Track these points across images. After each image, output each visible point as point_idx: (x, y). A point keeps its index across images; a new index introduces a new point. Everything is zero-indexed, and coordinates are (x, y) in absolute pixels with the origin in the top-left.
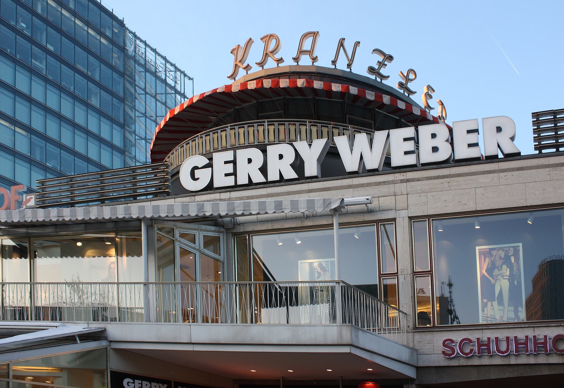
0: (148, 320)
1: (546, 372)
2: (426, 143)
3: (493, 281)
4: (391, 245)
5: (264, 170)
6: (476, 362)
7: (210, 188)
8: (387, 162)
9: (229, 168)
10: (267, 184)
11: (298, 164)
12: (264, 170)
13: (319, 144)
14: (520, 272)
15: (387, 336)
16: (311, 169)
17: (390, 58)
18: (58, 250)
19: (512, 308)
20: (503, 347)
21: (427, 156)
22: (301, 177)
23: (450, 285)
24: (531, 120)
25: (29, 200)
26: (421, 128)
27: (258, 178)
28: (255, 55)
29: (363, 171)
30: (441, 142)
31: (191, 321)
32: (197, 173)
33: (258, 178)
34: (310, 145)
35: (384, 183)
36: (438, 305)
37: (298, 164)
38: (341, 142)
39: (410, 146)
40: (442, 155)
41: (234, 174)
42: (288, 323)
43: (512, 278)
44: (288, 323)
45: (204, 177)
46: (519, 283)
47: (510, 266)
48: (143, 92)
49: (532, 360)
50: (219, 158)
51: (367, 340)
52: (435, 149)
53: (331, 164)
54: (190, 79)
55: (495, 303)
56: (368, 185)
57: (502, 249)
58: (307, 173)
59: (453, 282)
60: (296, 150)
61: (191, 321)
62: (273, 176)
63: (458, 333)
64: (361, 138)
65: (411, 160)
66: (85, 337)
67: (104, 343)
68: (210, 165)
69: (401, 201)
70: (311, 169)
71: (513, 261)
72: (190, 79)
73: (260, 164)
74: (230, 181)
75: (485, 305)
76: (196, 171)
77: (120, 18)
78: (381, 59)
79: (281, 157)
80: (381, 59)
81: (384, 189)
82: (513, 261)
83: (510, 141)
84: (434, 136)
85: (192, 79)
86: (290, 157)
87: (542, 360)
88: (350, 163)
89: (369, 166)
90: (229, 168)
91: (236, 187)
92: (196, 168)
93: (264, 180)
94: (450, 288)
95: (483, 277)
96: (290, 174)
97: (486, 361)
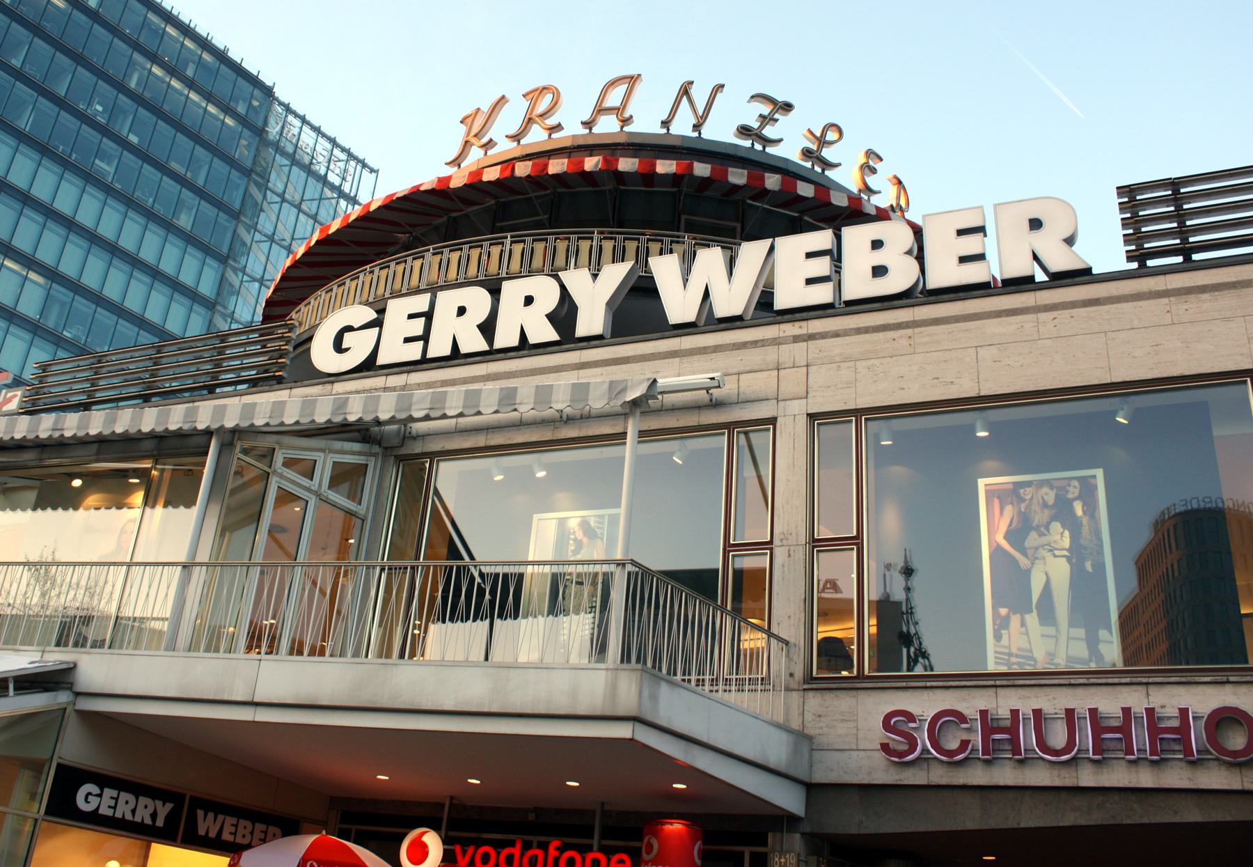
0: (172, 647)
1: (1192, 814)
3: (1023, 562)
4: (759, 477)
5: (487, 328)
6: (978, 776)
7: (369, 366)
10: (492, 354)
11: (565, 315)
12: (487, 328)
13: (615, 274)
14: (1101, 540)
15: (733, 697)
16: (591, 320)
17: (787, 107)
18: (32, 496)
19: (1080, 632)
20: (1058, 737)
21: (857, 284)
23: (908, 572)
24: (1114, 201)
25: (10, 400)
26: (847, 232)
28: (509, 120)
29: (708, 321)
31: (264, 649)
33: (473, 342)
34: (595, 276)
35: (755, 344)
36: (874, 621)
37: (565, 315)
38: (665, 269)
39: (822, 266)
42: (487, 659)
43: (1076, 555)
44: (487, 659)
45: (359, 346)
46: (1099, 567)
47: (1072, 525)
48: (278, 199)
49: (1145, 778)
50: (398, 310)
51: (681, 707)
52: (879, 271)
53: (638, 311)
54: (372, 171)
55: (1032, 619)
56: (717, 349)
57: (1048, 483)
58: (581, 330)
59: (915, 564)
60: (563, 288)
61: (264, 649)
62: (506, 337)
63: (926, 695)
64: (710, 259)
65: (823, 294)
66: (28, 682)
67: (63, 697)
69: (792, 381)
70: (591, 320)
71: (1079, 512)
72: (372, 171)
73: (482, 316)
75: (1002, 624)
76: (347, 336)
77: (269, 83)
78: (766, 109)
80: (766, 109)
81: (754, 357)
82: (1079, 512)
83: (1065, 246)
85: (377, 172)
87: (1176, 777)
88: (679, 304)
89: (721, 311)
91: (424, 362)
92: (349, 329)
93: (485, 347)
94: (907, 580)
95: (996, 552)
96: (543, 332)
97: (1006, 775)
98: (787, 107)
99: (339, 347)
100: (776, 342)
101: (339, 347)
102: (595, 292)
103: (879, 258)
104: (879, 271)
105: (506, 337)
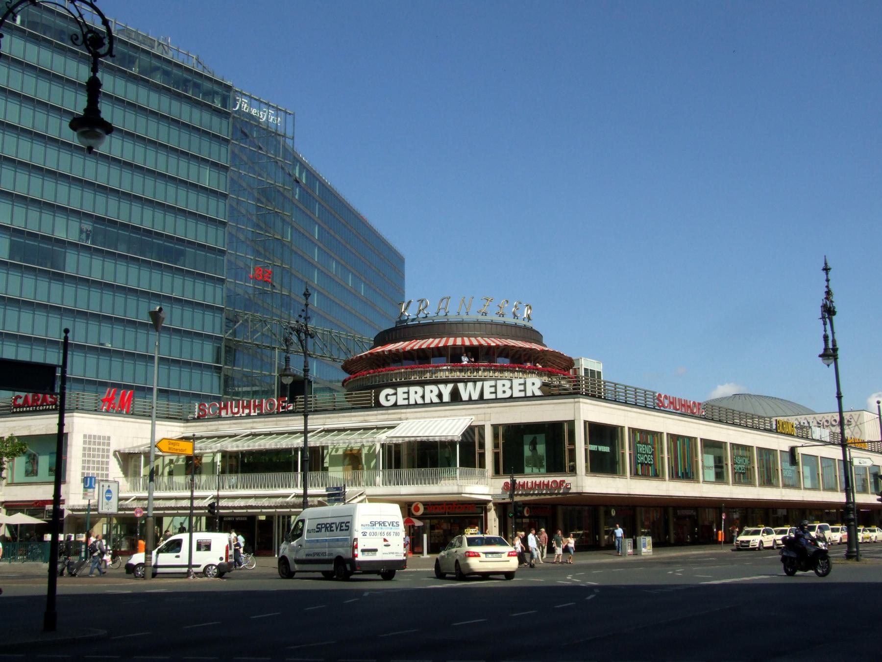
2: (500, 389)
7: (395, 406)
9: (406, 396)
10: (424, 405)
11: (440, 396)
12: (423, 397)
13: (450, 386)
16: (446, 398)
21: (500, 395)
22: (442, 403)
29: (470, 401)
30: (507, 388)
32: (389, 398)
33: (420, 401)
37: (440, 396)
40: (508, 395)
41: (408, 399)
45: (392, 400)
53: (456, 397)
62: (427, 401)
68: (395, 394)
74: (406, 402)
79: (432, 391)
81: (480, 411)
84: (504, 385)
86: (436, 392)
88: (465, 397)
90: (406, 396)
99: (388, 400)
101: (388, 400)
102: (447, 390)
103: (504, 389)
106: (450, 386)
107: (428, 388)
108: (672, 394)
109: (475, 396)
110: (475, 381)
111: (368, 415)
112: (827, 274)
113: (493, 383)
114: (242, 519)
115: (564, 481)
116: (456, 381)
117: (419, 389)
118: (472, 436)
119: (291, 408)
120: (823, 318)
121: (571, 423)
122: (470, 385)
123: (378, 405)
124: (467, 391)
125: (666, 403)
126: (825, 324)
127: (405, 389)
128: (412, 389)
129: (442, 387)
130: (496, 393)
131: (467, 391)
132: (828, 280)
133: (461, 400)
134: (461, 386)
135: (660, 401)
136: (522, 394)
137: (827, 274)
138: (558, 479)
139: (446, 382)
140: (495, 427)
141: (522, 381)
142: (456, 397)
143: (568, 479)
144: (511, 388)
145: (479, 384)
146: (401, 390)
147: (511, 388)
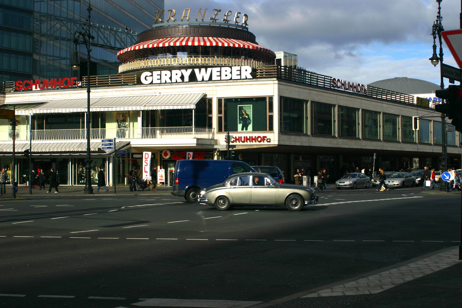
1: (255, 147)
2: (223, 73)
5: (171, 78)
7: (152, 83)
8: (210, 79)
11: (182, 77)
12: (171, 78)
13: (190, 71)
16: (186, 79)
21: (223, 77)
27: (169, 81)
30: (228, 73)
32: (147, 77)
37: (182, 77)
40: (229, 77)
45: (150, 80)
52: (226, 75)
53: (193, 78)
68: (152, 76)
70: (186, 79)
76: (147, 77)
79: (177, 74)
84: (226, 71)
88: (199, 78)
92: (147, 76)
96: (180, 80)
98: (220, 11)
100: (212, 86)
102: (187, 73)
103: (226, 73)
104: (226, 75)
105: (174, 81)
106: (190, 71)
107: (174, 72)
108: (343, 79)
109: (206, 78)
110: (206, 67)
111: (133, 90)
112: (439, 4)
113: (218, 69)
114: (47, 160)
115: (266, 137)
116: (193, 67)
117: (168, 73)
118: (204, 104)
119: (80, 85)
120: (434, 33)
121: (271, 98)
122: (203, 70)
123: (139, 83)
124: (201, 74)
125: (339, 84)
126: (435, 38)
127: (159, 72)
128: (164, 72)
129: (183, 71)
130: (220, 76)
131: (201, 74)
132: (439, 8)
133: (197, 81)
134: (197, 71)
135: (335, 83)
136: (239, 77)
137: (439, 4)
138: (262, 135)
139: (186, 68)
140: (220, 100)
141: (238, 68)
142: (193, 78)
143: (268, 135)
144: (231, 73)
145: (209, 70)
146: (156, 73)
147: (231, 73)
